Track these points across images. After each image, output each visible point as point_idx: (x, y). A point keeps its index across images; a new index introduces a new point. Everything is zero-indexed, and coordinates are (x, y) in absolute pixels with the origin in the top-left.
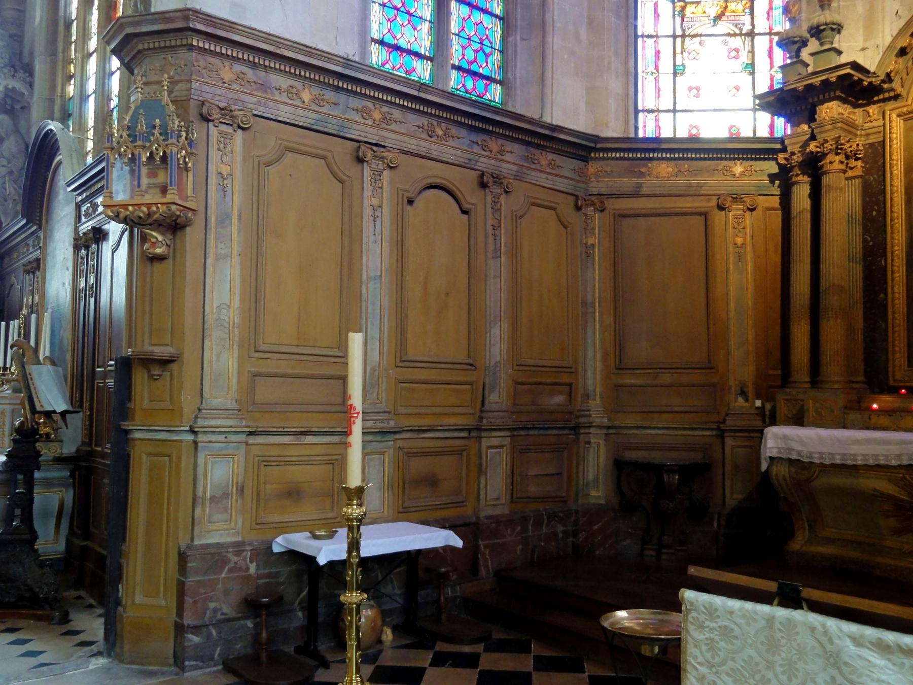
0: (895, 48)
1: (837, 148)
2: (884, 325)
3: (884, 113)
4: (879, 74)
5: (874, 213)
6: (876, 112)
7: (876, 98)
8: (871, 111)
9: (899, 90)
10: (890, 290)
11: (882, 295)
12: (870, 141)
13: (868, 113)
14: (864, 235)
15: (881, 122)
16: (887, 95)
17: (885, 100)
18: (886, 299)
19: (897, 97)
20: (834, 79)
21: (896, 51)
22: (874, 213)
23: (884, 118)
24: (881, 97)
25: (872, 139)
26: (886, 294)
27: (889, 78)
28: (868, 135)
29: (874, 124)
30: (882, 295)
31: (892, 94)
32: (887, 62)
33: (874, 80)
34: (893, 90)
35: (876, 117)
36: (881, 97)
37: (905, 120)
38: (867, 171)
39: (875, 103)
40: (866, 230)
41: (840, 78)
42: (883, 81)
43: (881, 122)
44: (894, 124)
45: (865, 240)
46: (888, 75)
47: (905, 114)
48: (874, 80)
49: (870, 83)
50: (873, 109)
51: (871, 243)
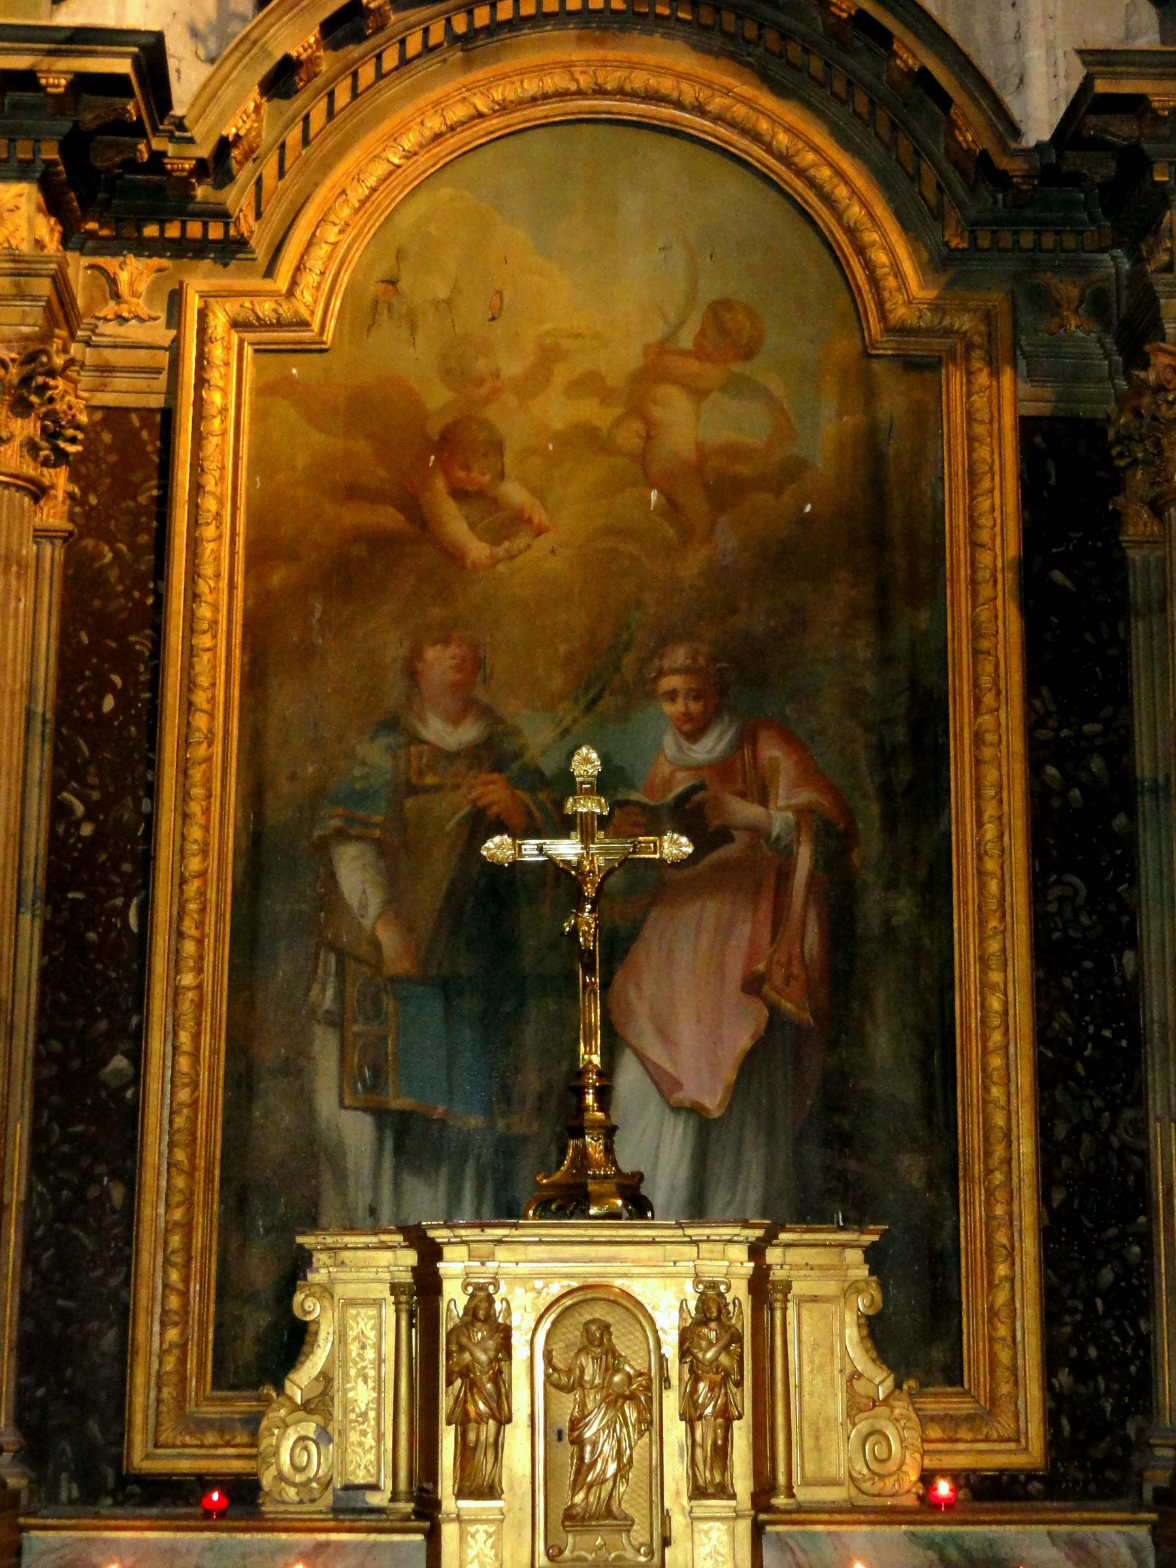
0: (269, 55)
1: (26, 380)
2: (117, 1194)
3: (176, 301)
4: (196, 132)
5: (109, 703)
6: (143, 287)
7: (151, 231)
8: (124, 277)
9: (247, 224)
10: (156, 1043)
11: (120, 1062)
12: (107, 399)
13: (113, 281)
14: (57, 786)
15: (162, 335)
16: (195, 229)
17: (186, 249)
18: (138, 1078)
19: (231, 250)
20: (57, 83)
21: (265, 68)
22: (109, 703)
23: (175, 317)
24: (173, 231)
25: (122, 393)
26: (138, 1057)
27: (219, 164)
28: (106, 370)
29: (133, 331)
30: (120, 1062)
31: (216, 232)
32: (228, 93)
33: (171, 149)
34: (222, 215)
35: (141, 306)
36: (173, 231)
37: (256, 351)
38: (88, 521)
39: (144, 248)
40: (66, 768)
41: (83, 82)
42: (202, 169)
43: (162, 335)
44: (217, 352)
45: (59, 811)
46: (224, 146)
47: (262, 325)
48: (171, 149)
49: (158, 157)
50: (133, 272)
51: (87, 830)
